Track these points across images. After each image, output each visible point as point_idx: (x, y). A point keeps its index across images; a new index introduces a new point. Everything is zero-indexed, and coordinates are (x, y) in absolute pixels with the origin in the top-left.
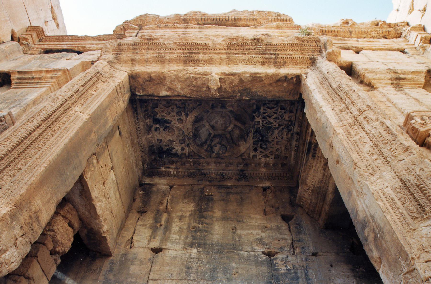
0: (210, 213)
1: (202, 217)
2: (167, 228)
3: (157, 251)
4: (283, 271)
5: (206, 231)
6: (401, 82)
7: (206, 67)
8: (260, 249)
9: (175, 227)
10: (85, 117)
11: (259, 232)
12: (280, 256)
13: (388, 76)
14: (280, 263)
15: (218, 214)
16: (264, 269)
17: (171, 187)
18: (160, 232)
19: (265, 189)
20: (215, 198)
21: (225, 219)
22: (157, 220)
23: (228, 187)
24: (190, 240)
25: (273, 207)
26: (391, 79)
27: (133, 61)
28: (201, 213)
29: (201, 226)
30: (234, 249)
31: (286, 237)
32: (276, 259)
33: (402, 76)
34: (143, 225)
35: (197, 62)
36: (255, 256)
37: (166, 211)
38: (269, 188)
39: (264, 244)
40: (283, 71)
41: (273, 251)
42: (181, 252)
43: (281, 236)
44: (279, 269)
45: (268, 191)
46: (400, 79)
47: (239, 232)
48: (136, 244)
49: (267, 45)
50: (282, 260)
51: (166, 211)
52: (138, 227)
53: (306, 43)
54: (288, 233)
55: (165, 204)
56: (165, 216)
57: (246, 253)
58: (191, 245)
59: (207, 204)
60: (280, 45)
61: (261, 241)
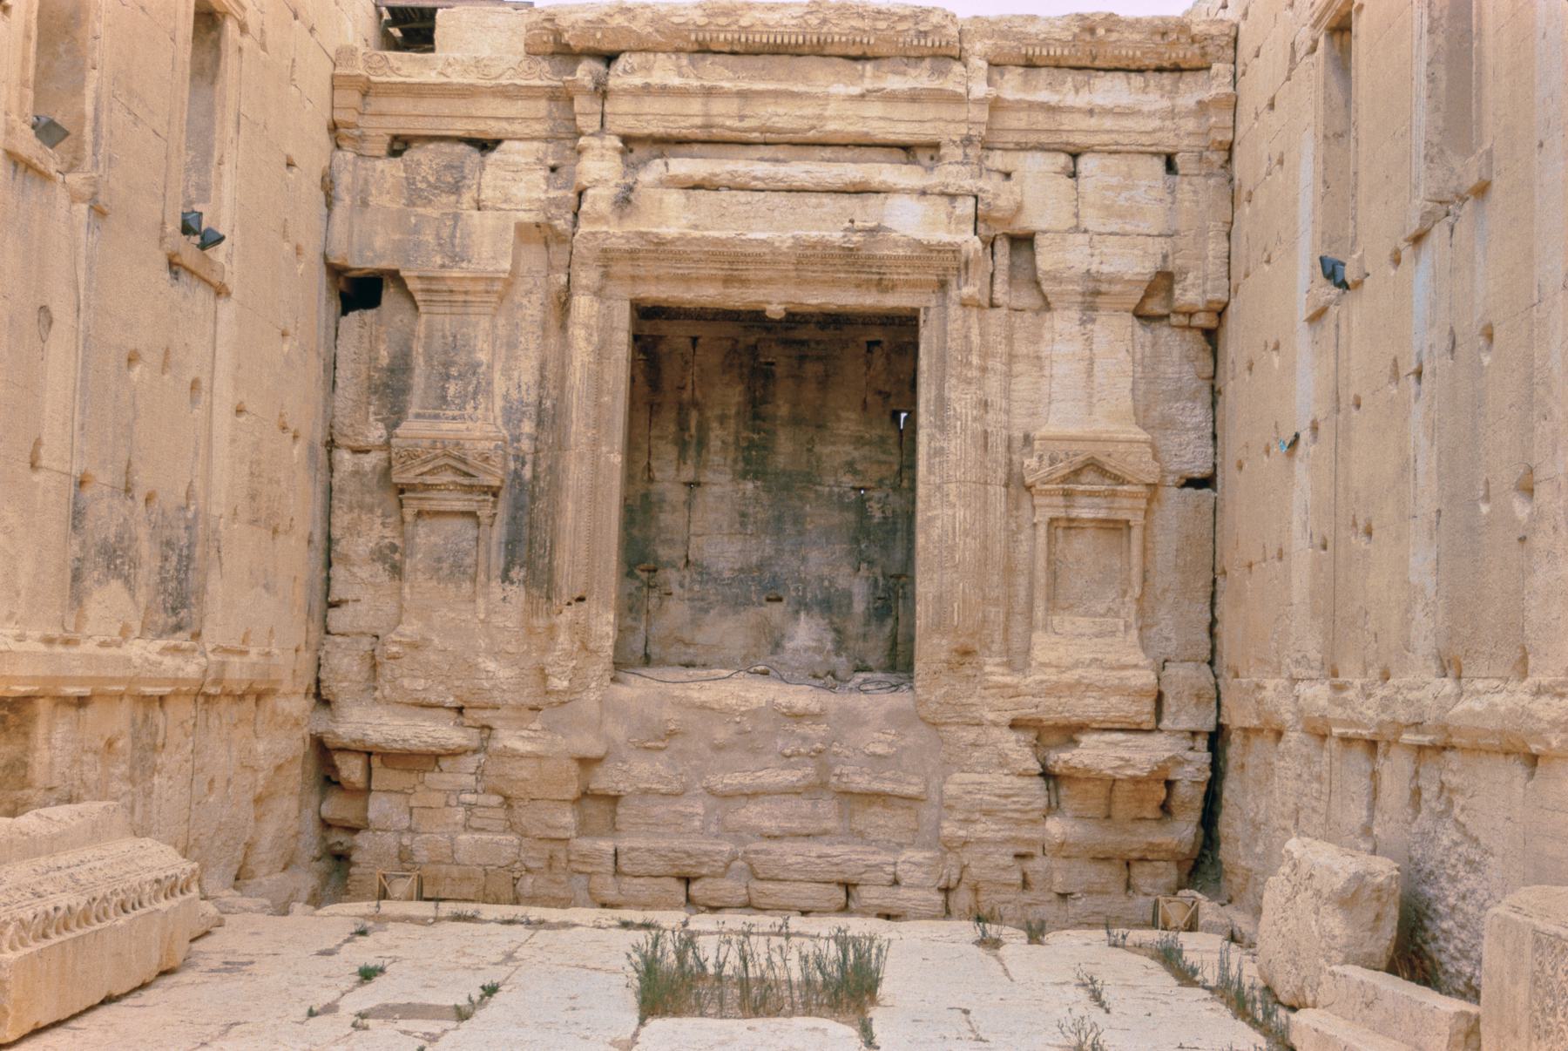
0: (769, 408)
1: (756, 416)
2: (702, 443)
3: (693, 485)
5: (765, 448)
7: (762, 291)
8: (848, 480)
9: (715, 443)
10: (617, 459)
11: (849, 448)
12: (876, 494)
13: (1079, 289)
14: (876, 506)
15: (784, 410)
16: (851, 516)
17: (695, 340)
18: (692, 452)
19: (872, 344)
20: (780, 371)
21: (796, 421)
22: (683, 426)
23: (802, 343)
24: (740, 466)
25: (880, 393)
26: (1083, 294)
27: (633, 278)
28: (756, 410)
29: (756, 436)
30: (810, 481)
31: (891, 459)
32: (870, 499)
33: (1104, 287)
34: (660, 438)
35: (744, 282)
36: (840, 496)
37: (695, 404)
38: (878, 343)
39: (855, 472)
42: (729, 488)
43: (882, 457)
44: (872, 517)
45: (877, 351)
46: (1098, 293)
47: (817, 449)
48: (658, 475)
49: (868, 257)
51: (695, 404)
52: (653, 442)
54: (896, 451)
55: (690, 387)
58: (744, 475)
59: (764, 387)
60: (890, 257)
61: (851, 467)
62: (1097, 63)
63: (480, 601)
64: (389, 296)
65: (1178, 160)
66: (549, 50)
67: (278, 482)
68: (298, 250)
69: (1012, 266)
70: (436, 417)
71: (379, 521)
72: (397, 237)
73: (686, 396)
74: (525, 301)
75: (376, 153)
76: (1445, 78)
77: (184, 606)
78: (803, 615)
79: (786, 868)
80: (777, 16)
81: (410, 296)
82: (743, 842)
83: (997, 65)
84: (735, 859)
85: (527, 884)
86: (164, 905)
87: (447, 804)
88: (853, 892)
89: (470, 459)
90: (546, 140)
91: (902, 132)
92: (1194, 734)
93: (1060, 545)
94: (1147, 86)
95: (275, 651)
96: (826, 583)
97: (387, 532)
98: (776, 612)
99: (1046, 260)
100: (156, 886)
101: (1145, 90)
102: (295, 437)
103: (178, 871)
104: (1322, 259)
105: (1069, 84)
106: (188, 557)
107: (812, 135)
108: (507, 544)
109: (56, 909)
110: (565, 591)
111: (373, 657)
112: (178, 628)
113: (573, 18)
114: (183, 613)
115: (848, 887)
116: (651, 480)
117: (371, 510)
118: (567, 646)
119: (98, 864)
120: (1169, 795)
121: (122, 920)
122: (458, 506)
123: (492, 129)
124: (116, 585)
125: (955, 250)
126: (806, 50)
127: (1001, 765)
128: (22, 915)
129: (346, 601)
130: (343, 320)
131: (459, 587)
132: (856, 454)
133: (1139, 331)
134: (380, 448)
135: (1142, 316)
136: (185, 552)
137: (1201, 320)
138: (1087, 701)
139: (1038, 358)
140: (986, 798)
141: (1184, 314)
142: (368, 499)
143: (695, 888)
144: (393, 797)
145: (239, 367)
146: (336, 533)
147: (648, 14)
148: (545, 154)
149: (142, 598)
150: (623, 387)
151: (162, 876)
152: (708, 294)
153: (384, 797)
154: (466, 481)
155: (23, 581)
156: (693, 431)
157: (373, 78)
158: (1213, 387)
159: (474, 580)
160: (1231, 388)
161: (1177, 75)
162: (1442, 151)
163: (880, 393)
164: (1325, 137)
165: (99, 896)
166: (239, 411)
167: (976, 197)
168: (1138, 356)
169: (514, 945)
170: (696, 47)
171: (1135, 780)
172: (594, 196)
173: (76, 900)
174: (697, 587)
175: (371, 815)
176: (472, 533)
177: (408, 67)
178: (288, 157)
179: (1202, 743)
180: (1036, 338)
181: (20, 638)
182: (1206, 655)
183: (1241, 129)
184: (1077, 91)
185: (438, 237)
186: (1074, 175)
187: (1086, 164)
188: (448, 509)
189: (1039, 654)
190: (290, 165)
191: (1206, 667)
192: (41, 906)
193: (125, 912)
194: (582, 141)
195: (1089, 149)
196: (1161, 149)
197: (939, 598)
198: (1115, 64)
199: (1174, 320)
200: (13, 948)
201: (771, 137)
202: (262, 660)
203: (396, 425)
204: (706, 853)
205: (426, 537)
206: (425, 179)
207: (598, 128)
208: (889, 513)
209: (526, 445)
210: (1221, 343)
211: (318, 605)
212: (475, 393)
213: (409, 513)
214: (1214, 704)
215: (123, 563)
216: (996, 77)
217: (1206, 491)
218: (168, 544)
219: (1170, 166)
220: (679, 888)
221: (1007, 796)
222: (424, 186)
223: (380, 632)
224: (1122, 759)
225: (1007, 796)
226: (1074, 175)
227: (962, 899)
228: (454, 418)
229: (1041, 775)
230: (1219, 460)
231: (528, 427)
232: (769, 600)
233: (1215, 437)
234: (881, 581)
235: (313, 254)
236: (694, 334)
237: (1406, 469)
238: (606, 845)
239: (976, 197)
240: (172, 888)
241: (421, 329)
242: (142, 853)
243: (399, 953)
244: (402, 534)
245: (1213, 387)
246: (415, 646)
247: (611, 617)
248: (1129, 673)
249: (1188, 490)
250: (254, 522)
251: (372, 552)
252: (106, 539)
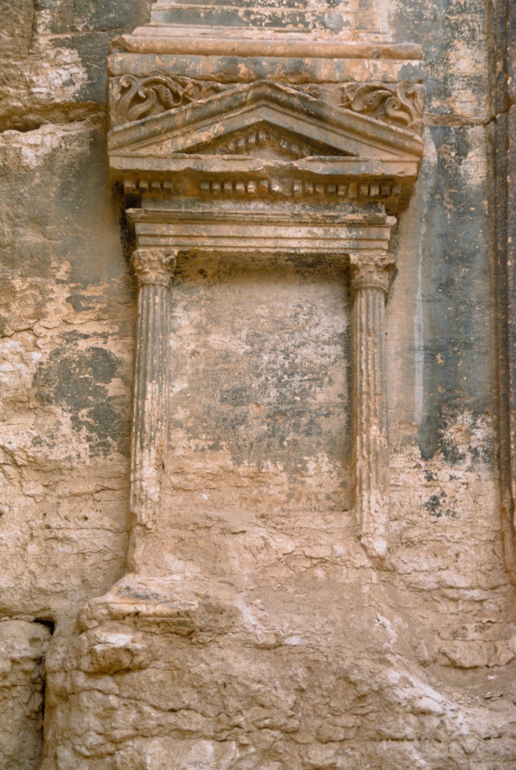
63: (372, 499)
71: (61, 294)
89: (333, 108)
97: (84, 324)
108: (431, 352)
111: (40, 685)
117: (41, 267)
122: (298, 238)
131: (297, 471)
134: (64, 112)
142: (31, 237)
154: (321, 167)
159: (346, 451)
176: (330, 322)
188: (268, 247)
205: (194, 331)
213: (153, 261)
223: (58, 606)
244: (133, 330)
251: (41, 376)
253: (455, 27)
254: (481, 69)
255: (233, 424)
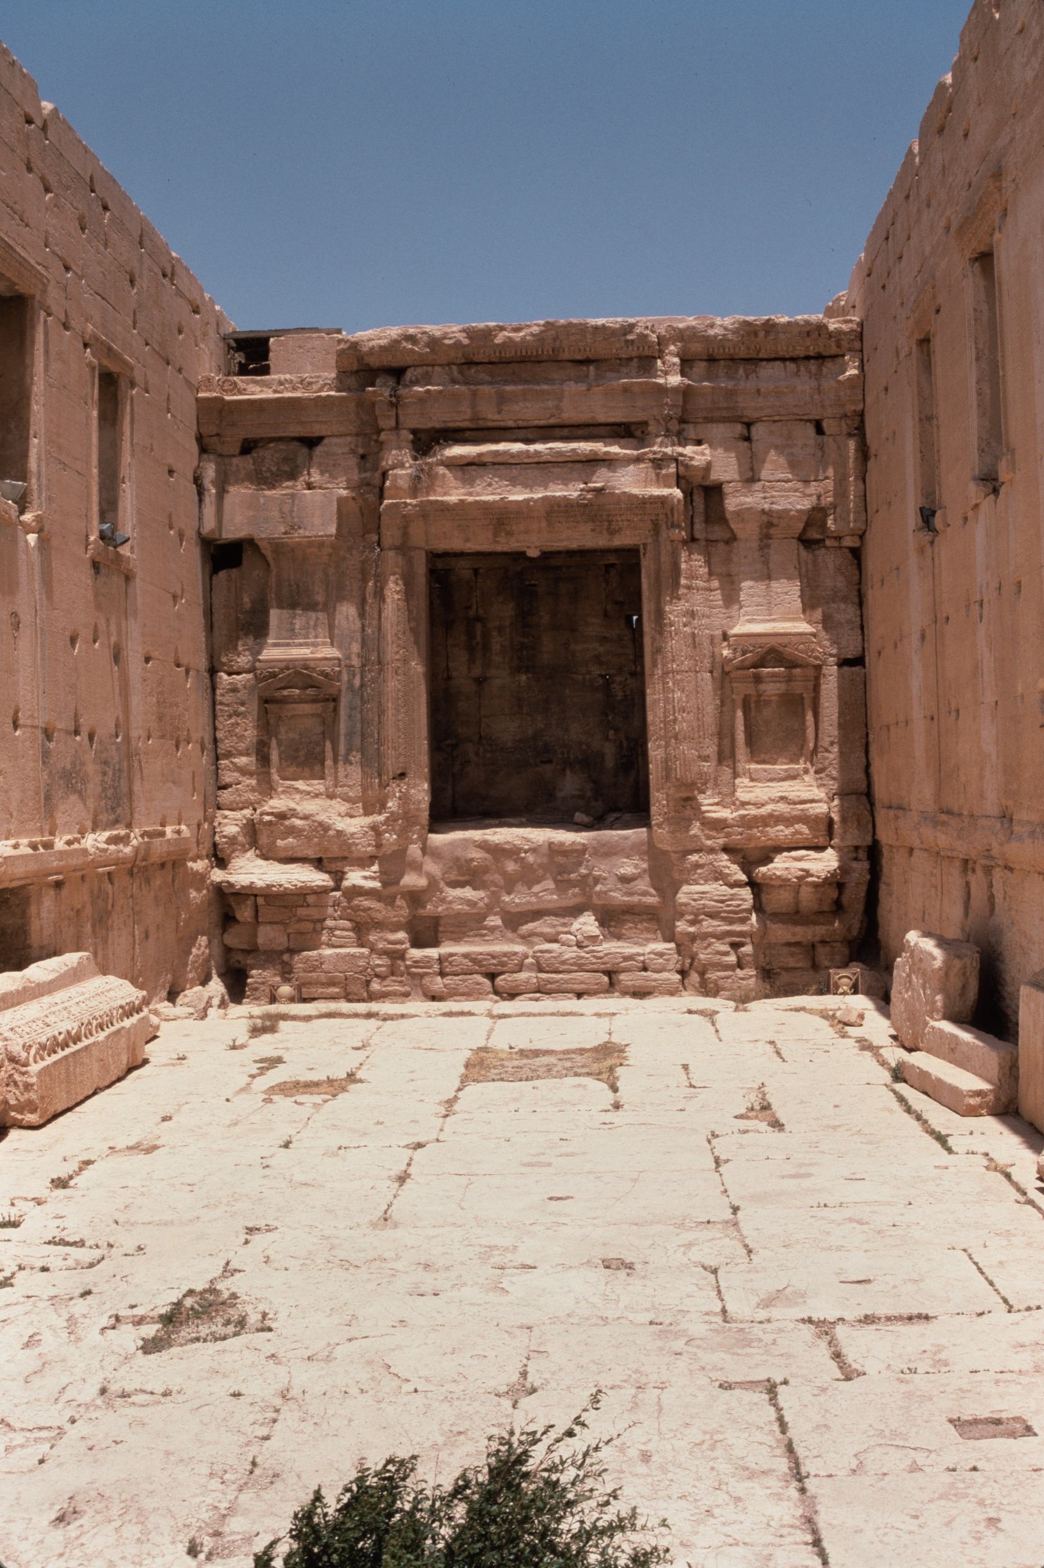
2: (486, 647)
3: (481, 681)
4: (619, 698)
6: (772, 531)
8: (596, 670)
9: (496, 647)
12: (618, 679)
15: (545, 619)
17: (476, 571)
19: (609, 567)
22: (470, 635)
25: (617, 603)
29: (526, 640)
32: (613, 683)
33: (775, 521)
35: (510, 534)
37: (478, 619)
38: (613, 565)
40: (618, 542)
41: (611, 672)
47: (572, 647)
48: (455, 674)
50: (620, 683)
53: (648, 506)
55: (475, 606)
56: (479, 626)
57: (581, 677)
58: (518, 670)
62: (761, 356)
64: (247, 557)
65: (825, 424)
66: (355, 368)
67: (176, 705)
68: (181, 535)
69: (707, 507)
70: (288, 645)
72: (251, 513)
73: (472, 613)
74: (348, 556)
75: (232, 452)
76: (989, 391)
77: (118, 805)
78: (568, 772)
79: (563, 963)
80: (521, 334)
81: (263, 557)
82: (531, 944)
83: (687, 360)
84: (527, 957)
85: (376, 986)
86: (127, 1023)
87: (314, 930)
88: (613, 976)
90: (357, 435)
91: (618, 415)
92: (857, 848)
93: (753, 714)
94: (798, 370)
95: (183, 827)
96: (584, 747)
98: (548, 770)
99: (732, 503)
100: (121, 1011)
101: (797, 374)
102: (187, 671)
103: (133, 999)
104: (921, 509)
105: (741, 371)
106: (120, 770)
107: (552, 421)
109: (60, 1033)
110: (390, 769)
112: (116, 822)
113: (371, 344)
114: (119, 811)
115: (609, 973)
116: (449, 678)
117: (245, 717)
118: (393, 809)
119: (82, 998)
120: (840, 894)
121: (101, 1036)
123: (317, 430)
124: (74, 798)
125: (662, 500)
126: (545, 358)
127: (716, 879)
128: (39, 1040)
129: (230, 786)
130: (215, 578)
132: (601, 649)
133: (804, 553)
135: (807, 542)
136: (117, 767)
137: (849, 542)
138: (778, 828)
139: (729, 575)
140: (707, 902)
141: (835, 538)
143: (500, 981)
144: (275, 927)
145: (145, 625)
146: (220, 735)
147: (425, 338)
148: (357, 446)
149: (91, 803)
150: (424, 615)
151: (123, 1003)
152: (481, 542)
153: (268, 928)
155: (13, 806)
156: (479, 639)
157: (227, 398)
158: (859, 590)
160: (873, 595)
161: (820, 361)
162: (989, 444)
163: (617, 603)
164: (920, 420)
165: (86, 1021)
166: (147, 660)
167: (676, 460)
168: (804, 570)
169: (369, 1034)
170: (463, 361)
171: (815, 885)
172: (396, 475)
173: (72, 1026)
174: (489, 755)
175: (260, 940)
177: (255, 390)
178: (169, 466)
179: (862, 854)
180: (728, 560)
181: (16, 846)
182: (863, 787)
183: (868, 400)
184: (747, 378)
185: (281, 511)
186: (748, 439)
187: (758, 431)
189: (742, 795)
190: (171, 472)
191: (864, 799)
192: (50, 1032)
193: (103, 1030)
194: (383, 436)
195: (759, 420)
196: (811, 417)
197: (666, 760)
198: (773, 356)
199: (828, 543)
200: (35, 1062)
201: (521, 424)
202: (176, 836)
203: (259, 653)
204: (505, 955)
206: (271, 471)
207: (393, 423)
208: (628, 693)
209: (356, 662)
210: (863, 557)
211: (211, 789)
212: (316, 626)
214: (870, 826)
215: (77, 782)
216: (687, 370)
217: (856, 669)
218: (106, 763)
219: (820, 430)
220: (487, 982)
221: (722, 902)
222: (268, 474)
224: (802, 870)
225: (722, 902)
226: (748, 439)
227: (694, 977)
228: (301, 645)
229: (747, 884)
230: (866, 645)
231: (356, 648)
232: (542, 762)
233: (862, 628)
234: (625, 744)
235: (191, 533)
236: (477, 566)
237: (976, 670)
238: (433, 952)
239: (676, 460)
240: (129, 1010)
241: (273, 580)
242: (108, 987)
243: (290, 1045)
245: (859, 590)
246: (282, 816)
247: (426, 786)
248: (808, 806)
249: (846, 668)
250: (163, 737)
252: (64, 768)
253: (352, 638)
254: (359, 650)
255: (295, 758)
